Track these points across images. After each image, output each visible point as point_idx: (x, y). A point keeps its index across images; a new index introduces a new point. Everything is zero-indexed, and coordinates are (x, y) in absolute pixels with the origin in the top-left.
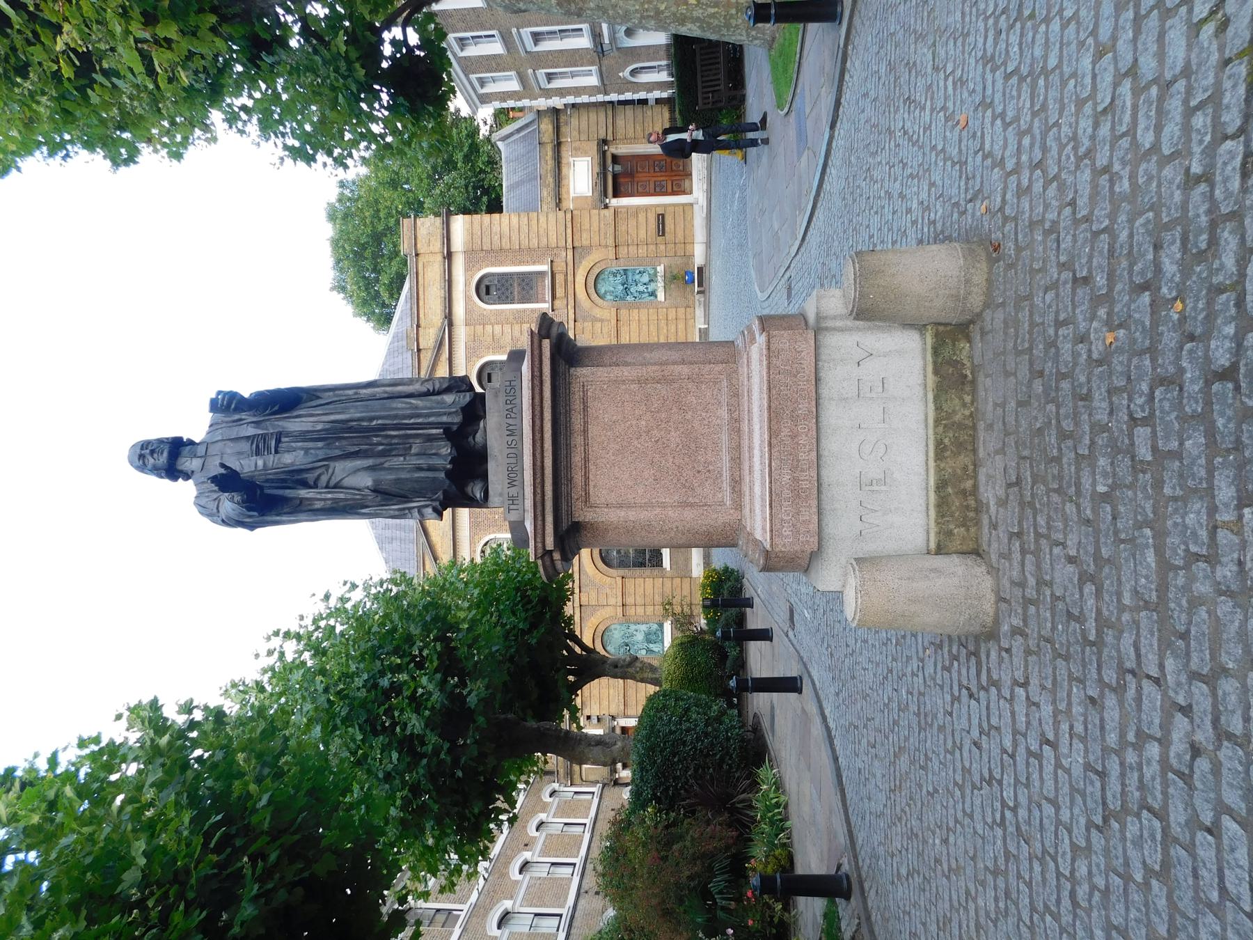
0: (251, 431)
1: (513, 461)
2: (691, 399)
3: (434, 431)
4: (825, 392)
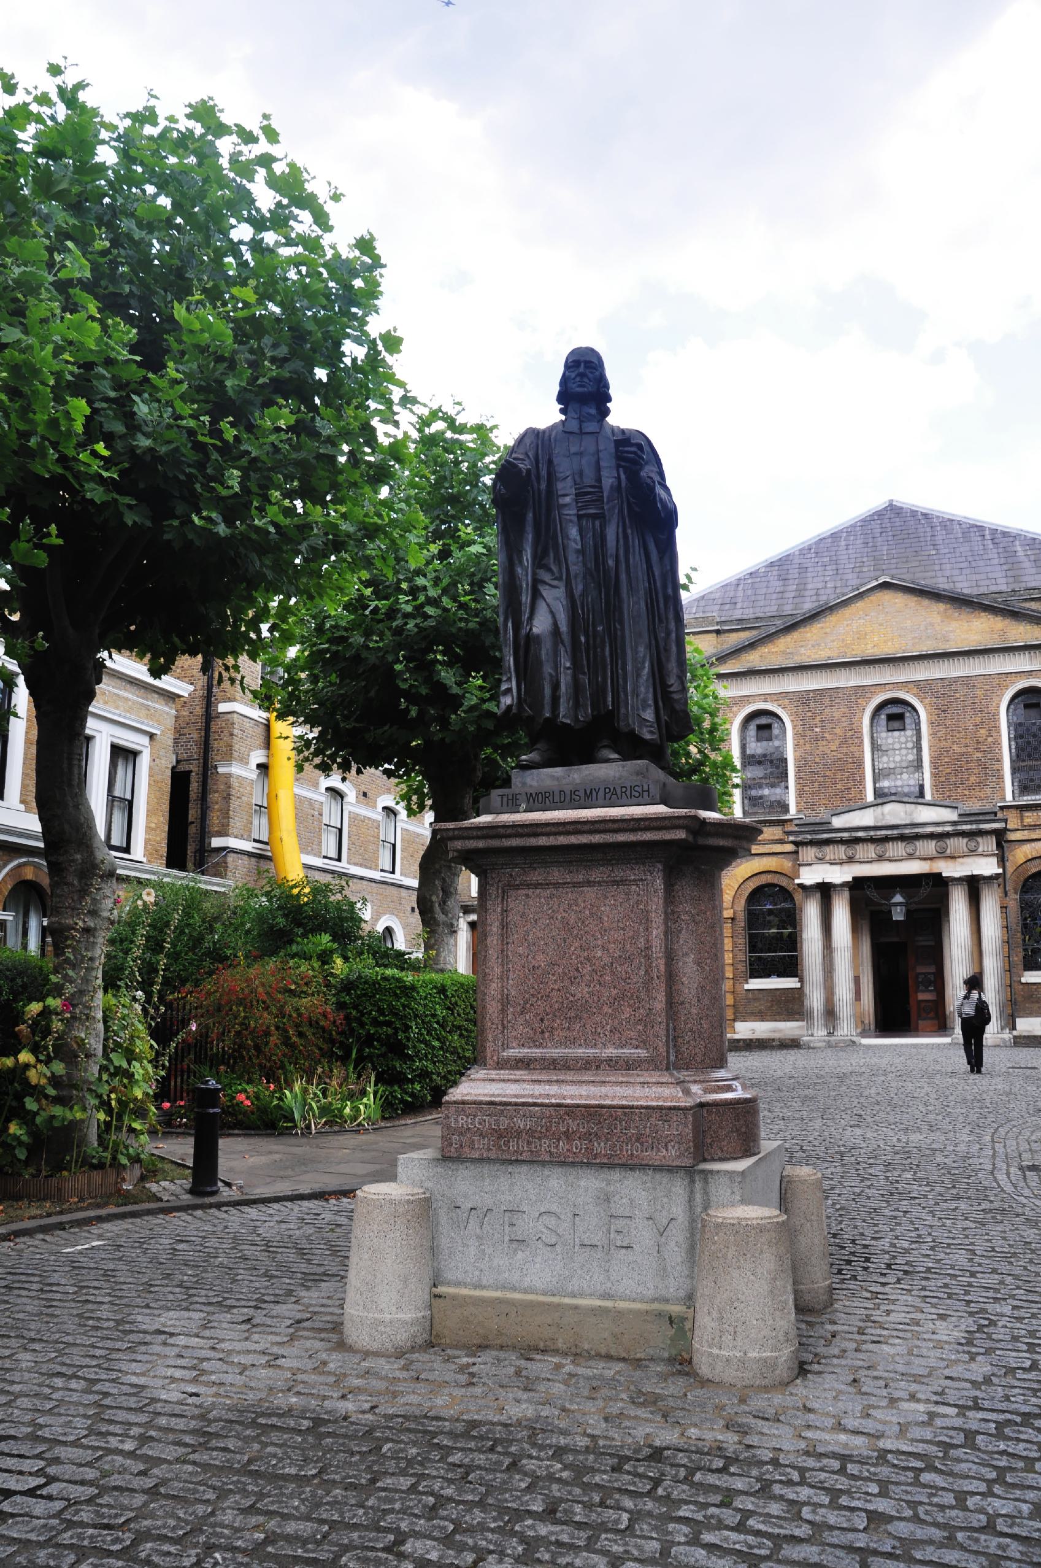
0: (608, 482)
1: (557, 799)
2: (627, 1012)
4: (616, 1175)
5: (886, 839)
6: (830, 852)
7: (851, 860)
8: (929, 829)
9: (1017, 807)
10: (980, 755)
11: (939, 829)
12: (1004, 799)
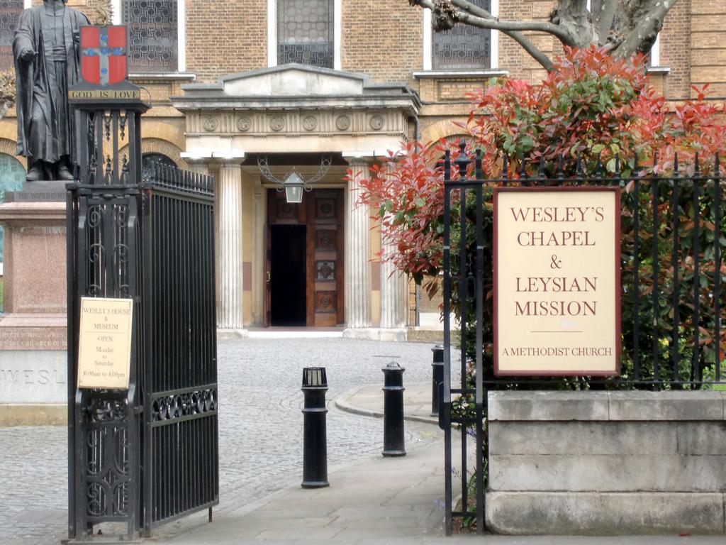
3: (68, 149)
5: (282, 113)
6: (222, 125)
7: (243, 134)
8: (332, 104)
9: (435, 78)
10: (398, 14)
11: (341, 104)
12: (421, 68)
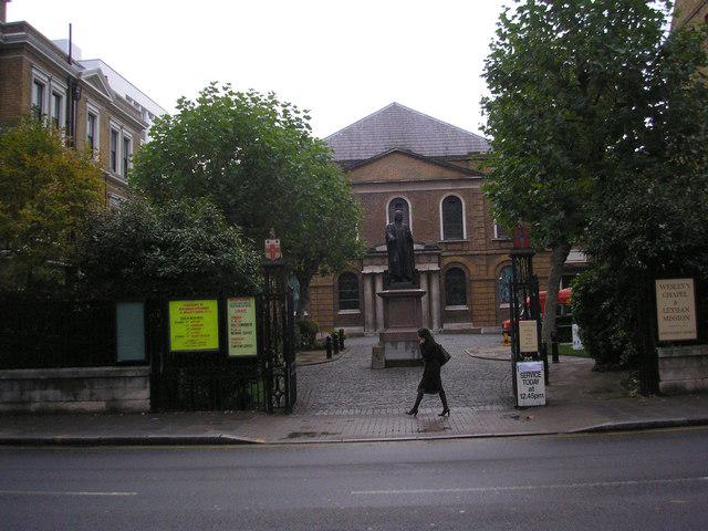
6: (375, 261)
